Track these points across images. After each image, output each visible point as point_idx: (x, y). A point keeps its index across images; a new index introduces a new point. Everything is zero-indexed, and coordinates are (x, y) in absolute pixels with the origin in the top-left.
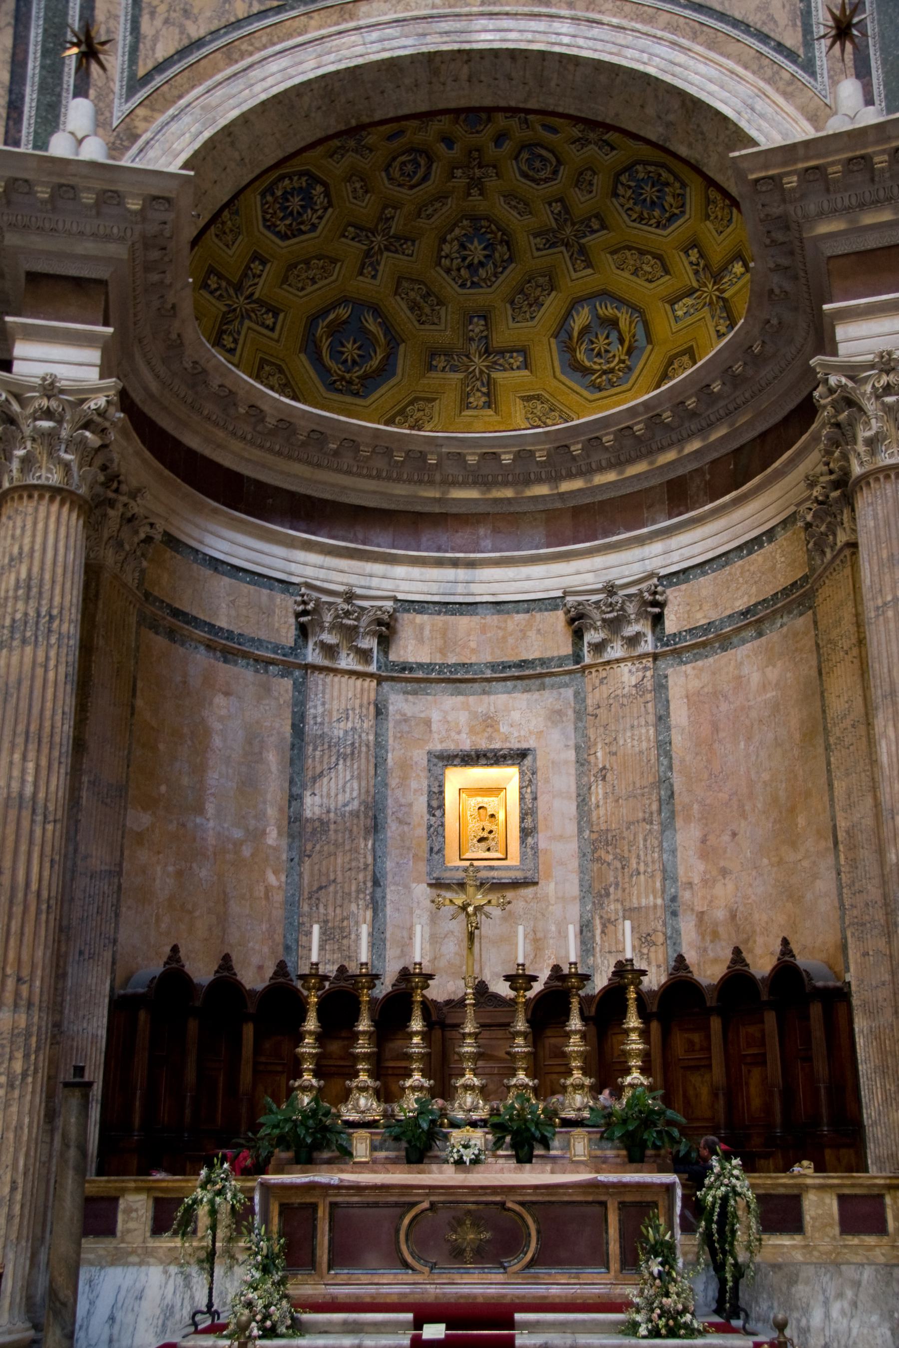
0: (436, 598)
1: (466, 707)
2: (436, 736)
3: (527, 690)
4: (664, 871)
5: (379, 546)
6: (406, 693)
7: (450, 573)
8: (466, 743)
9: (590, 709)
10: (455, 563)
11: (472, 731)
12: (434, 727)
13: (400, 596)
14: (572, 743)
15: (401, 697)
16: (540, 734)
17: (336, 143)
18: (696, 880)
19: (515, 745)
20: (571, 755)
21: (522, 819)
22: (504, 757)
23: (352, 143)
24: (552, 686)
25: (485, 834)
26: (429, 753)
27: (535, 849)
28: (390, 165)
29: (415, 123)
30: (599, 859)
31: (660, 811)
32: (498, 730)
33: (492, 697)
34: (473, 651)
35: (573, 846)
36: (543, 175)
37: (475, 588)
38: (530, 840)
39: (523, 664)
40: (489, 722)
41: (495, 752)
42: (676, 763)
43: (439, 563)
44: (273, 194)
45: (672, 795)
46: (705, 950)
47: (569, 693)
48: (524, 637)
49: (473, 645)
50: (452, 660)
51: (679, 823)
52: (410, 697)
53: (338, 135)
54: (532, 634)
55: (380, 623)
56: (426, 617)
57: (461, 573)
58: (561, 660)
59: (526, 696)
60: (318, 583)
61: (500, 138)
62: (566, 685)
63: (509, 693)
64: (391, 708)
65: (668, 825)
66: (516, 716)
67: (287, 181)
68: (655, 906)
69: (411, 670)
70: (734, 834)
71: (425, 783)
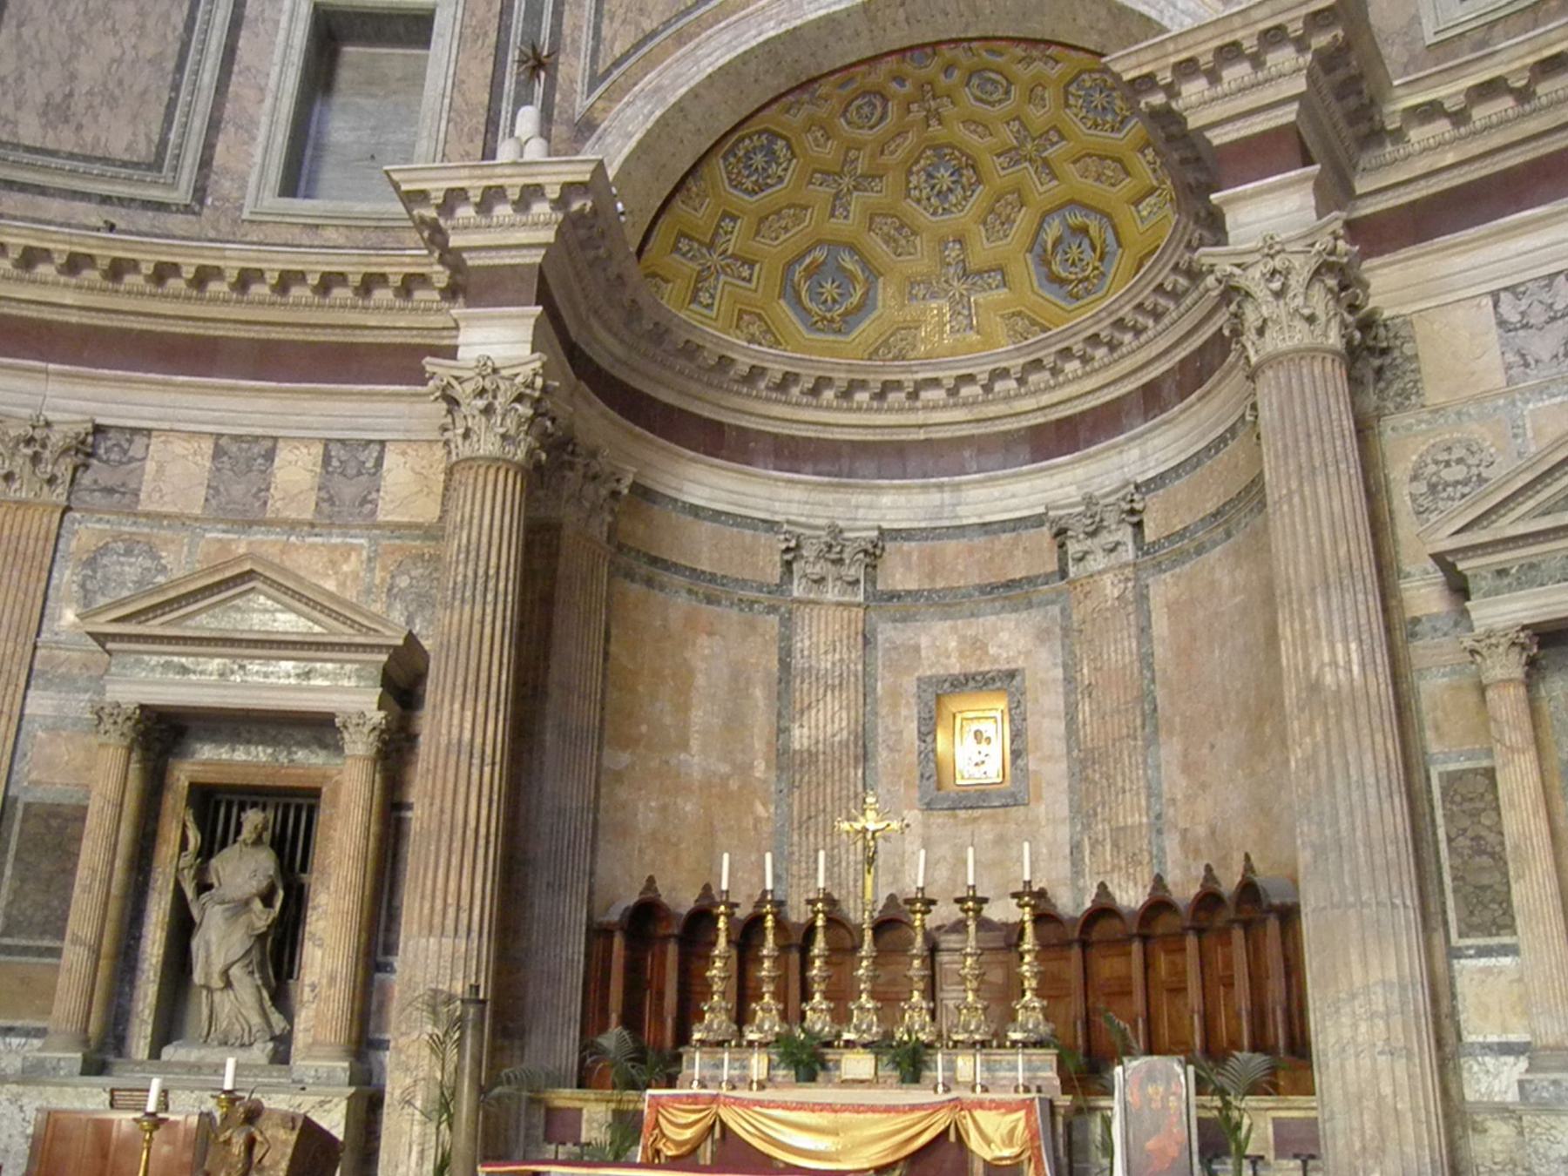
0: (923, 525)
1: (954, 629)
2: (926, 663)
3: (1015, 610)
4: (1149, 787)
5: (864, 477)
6: (895, 621)
7: (935, 498)
8: (955, 667)
9: (1076, 625)
10: (940, 487)
11: (962, 655)
12: (923, 653)
13: (885, 525)
14: (1059, 661)
15: (890, 625)
16: (1028, 654)
17: (791, 98)
18: (1179, 797)
19: (1005, 667)
20: (1059, 673)
21: (1012, 742)
22: (993, 679)
23: (806, 97)
24: (1040, 605)
25: (982, 757)
26: (919, 679)
27: (1025, 771)
28: (846, 111)
29: (864, 68)
30: (1087, 778)
31: (1143, 726)
32: (987, 653)
33: (981, 620)
34: (961, 574)
35: (1064, 766)
36: (996, 97)
37: (961, 510)
38: (1020, 762)
39: (1010, 584)
40: (977, 645)
41: (983, 674)
42: (1158, 674)
43: (924, 487)
44: (735, 155)
45: (1155, 710)
46: (1188, 868)
47: (1055, 610)
48: (1011, 555)
49: (961, 568)
50: (940, 584)
51: (1163, 737)
52: (899, 625)
53: (790, 91)
54: (1019, 553)
55: (866, 552)
56: (913, 544)
57: (947, 496)
58: (1047, 578)
59: (1014, 616)
60: (803, 519)
61: (948, 69)
62: (1053, 602)
63: (997, 613)
64: (880, 637)
65: (1152, 741)
66: (1004, 636)
67: (747, 142)
68: (1141, 824)
69: (899, 597)
70: (1212, 746)
71: (915, 711)
